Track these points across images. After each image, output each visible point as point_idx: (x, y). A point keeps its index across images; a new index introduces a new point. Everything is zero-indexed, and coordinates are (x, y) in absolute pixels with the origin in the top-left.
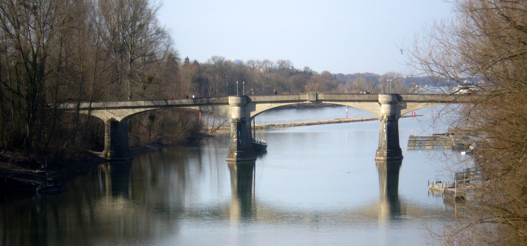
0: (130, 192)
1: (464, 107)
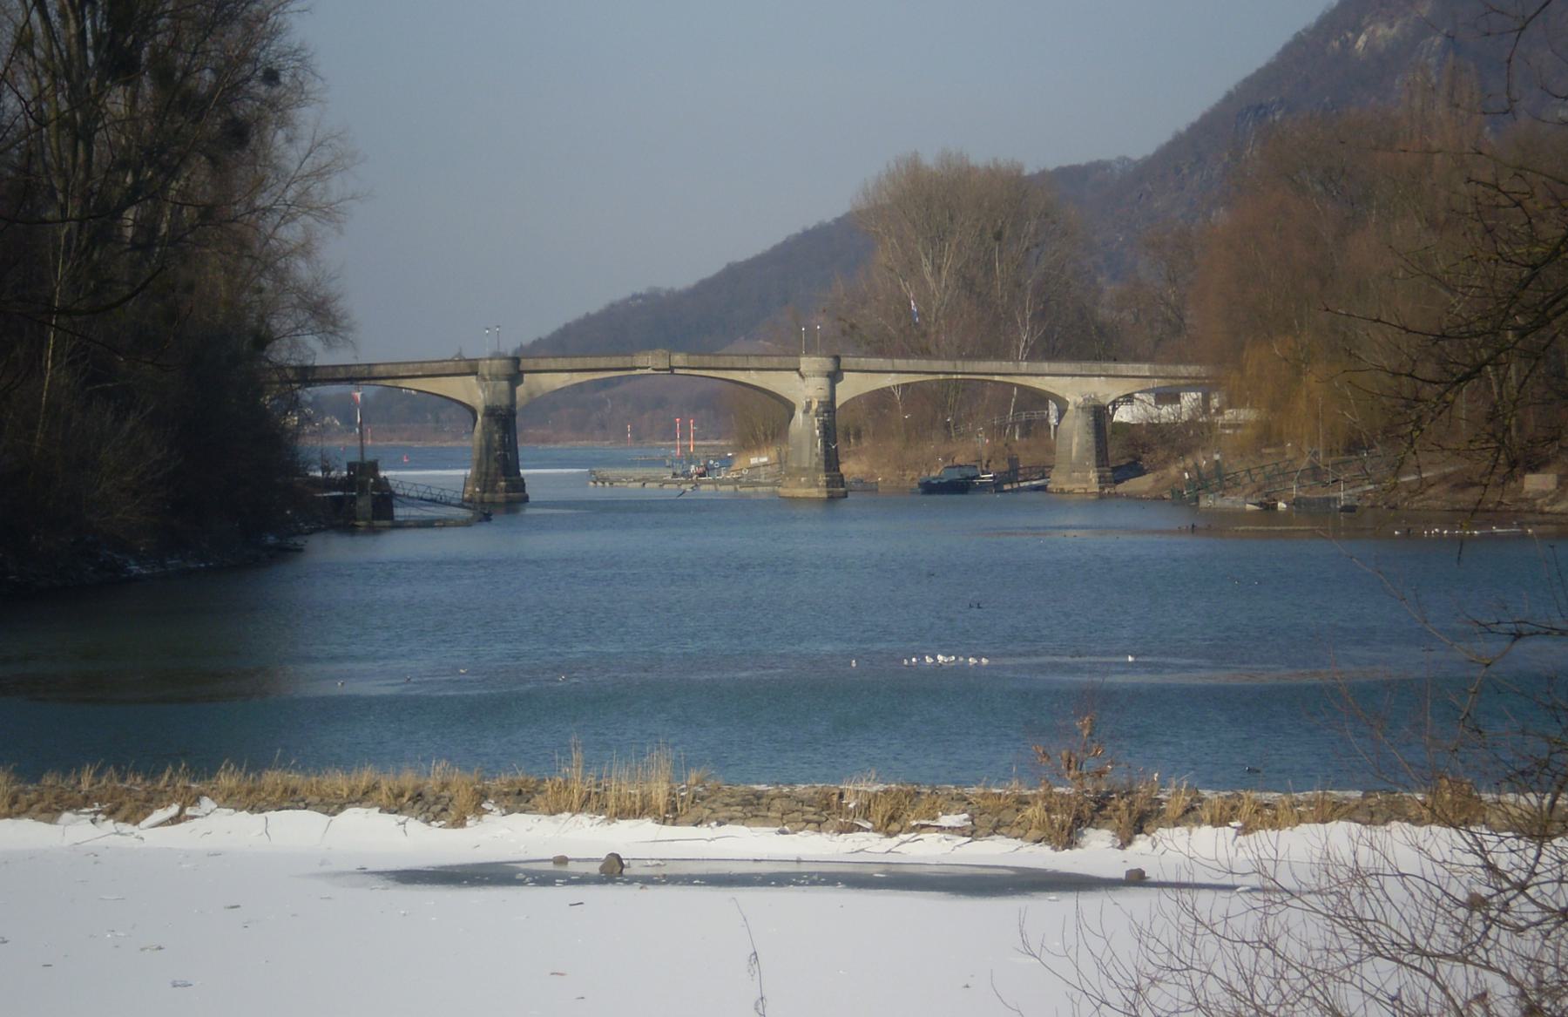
0: (244, 769)
1: (1085, 404)
